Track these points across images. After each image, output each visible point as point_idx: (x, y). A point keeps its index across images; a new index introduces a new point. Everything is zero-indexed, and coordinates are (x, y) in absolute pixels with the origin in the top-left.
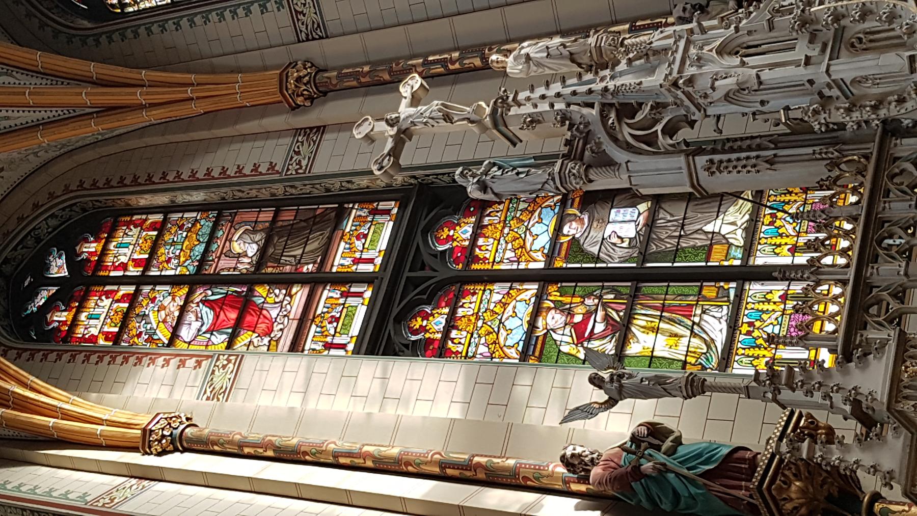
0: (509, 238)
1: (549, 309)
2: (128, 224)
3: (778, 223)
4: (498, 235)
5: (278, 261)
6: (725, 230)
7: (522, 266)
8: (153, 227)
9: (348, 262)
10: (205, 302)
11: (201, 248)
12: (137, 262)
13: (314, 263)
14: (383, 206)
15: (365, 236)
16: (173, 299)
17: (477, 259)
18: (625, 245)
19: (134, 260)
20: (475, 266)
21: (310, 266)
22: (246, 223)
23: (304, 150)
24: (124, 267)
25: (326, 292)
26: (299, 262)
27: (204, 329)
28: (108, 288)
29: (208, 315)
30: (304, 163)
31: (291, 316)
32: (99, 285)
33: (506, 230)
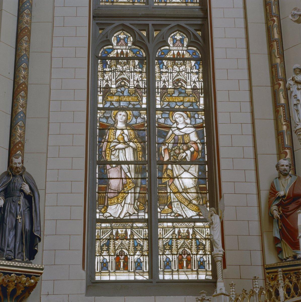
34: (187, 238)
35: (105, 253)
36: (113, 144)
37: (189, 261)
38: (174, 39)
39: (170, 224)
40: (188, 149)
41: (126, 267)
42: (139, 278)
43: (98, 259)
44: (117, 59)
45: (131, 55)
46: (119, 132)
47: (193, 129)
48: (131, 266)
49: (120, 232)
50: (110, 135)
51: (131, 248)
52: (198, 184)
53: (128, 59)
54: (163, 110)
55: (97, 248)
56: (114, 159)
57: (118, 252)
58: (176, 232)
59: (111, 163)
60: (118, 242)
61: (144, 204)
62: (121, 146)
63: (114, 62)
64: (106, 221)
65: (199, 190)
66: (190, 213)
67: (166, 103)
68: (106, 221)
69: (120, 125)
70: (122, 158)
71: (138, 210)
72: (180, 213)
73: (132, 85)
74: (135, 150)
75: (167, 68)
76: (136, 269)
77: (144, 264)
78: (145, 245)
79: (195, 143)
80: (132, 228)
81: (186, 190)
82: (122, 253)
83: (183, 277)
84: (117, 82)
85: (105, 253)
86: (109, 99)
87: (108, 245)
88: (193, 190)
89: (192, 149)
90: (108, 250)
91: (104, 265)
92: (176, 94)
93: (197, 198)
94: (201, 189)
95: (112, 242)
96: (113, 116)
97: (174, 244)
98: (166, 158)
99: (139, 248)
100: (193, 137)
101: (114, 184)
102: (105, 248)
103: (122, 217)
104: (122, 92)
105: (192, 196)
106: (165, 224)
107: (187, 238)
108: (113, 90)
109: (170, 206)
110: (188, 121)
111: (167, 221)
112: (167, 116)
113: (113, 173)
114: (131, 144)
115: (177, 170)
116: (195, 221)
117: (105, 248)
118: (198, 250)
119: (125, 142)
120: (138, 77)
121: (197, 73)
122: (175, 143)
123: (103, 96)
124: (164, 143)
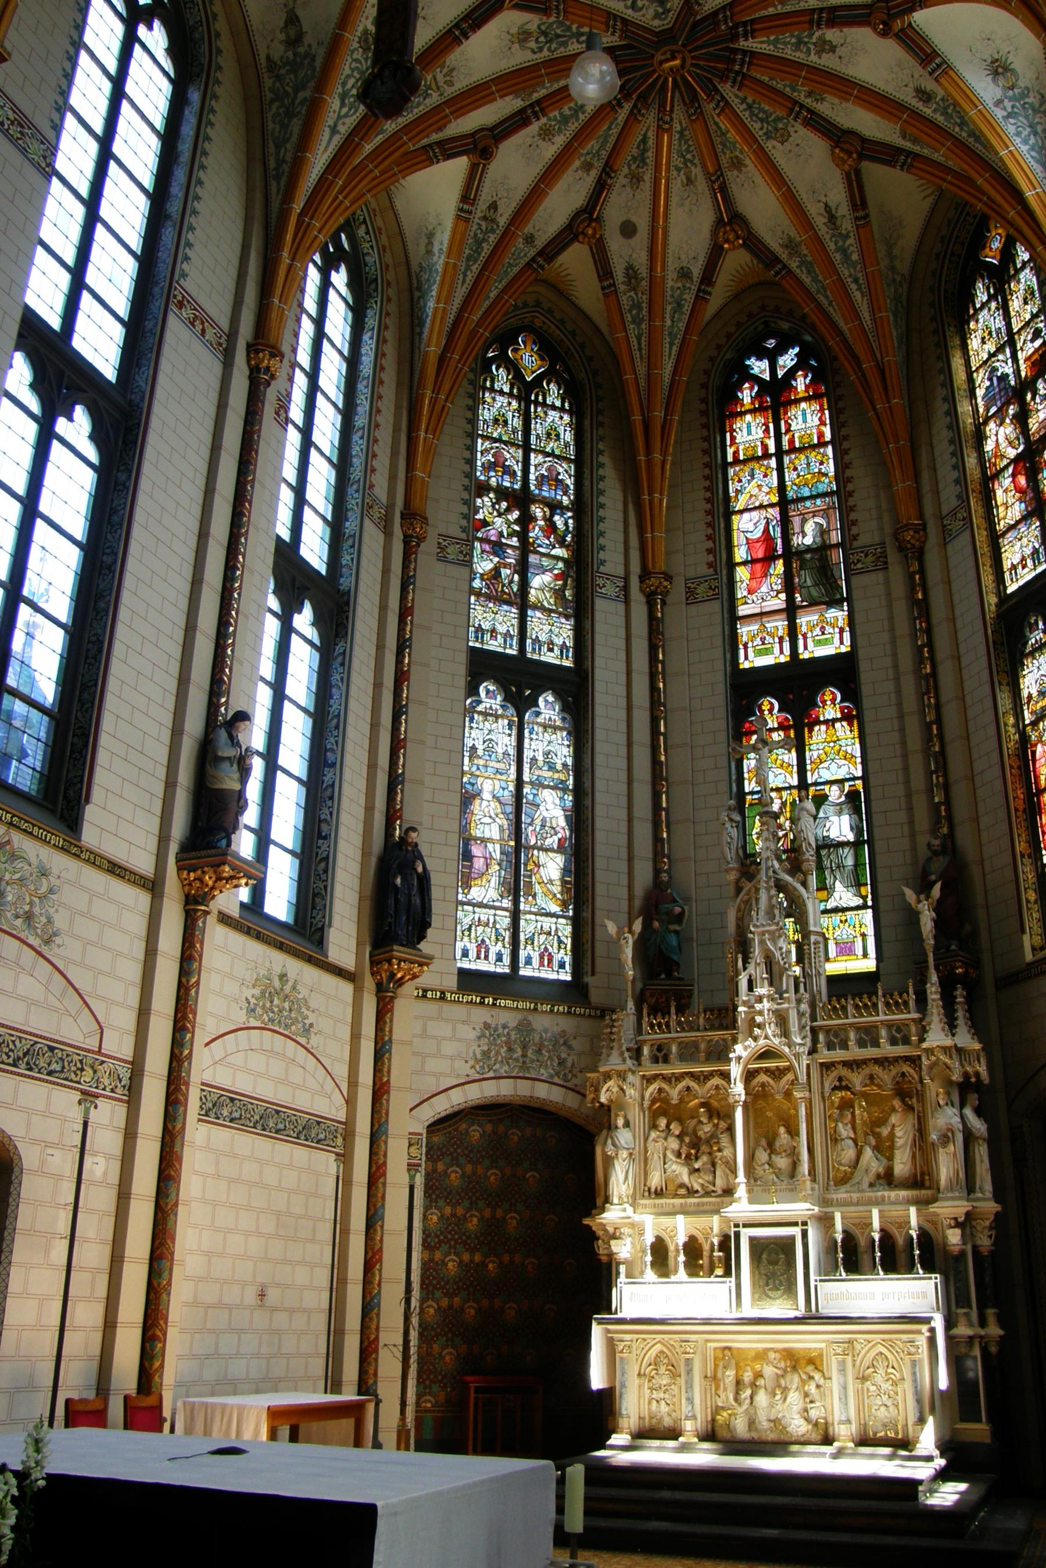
0: (827, 749)
1: (781, 798)
2: (822, 410)
3: (841, 925)
4: (829, 739)
5: (801, 568)
6: (836, 895)
7: (809, 767)
8: (821, 435)
9: (804, 629)
10: (767, 524)
11: (806, 492)
12: (792, 441)
13: (802, 601)
14: (847, 636)
15: (823, 633)
16: (767, 493)
17: (811, 731)
18: (825, 834)
19: (793, 436)
20: (806, 729)
21: (799, 599)
22: (828, 523)
23: (870, 558)
24: (788, 430)
25: (781, 623)
26: (801, 587)
27: (749, 535)
28: (771, 426)
29: (758, 534)
30: (859, 566)
31: (763, 604)
32: (773, 418)
33: (832, 744)
34: (549, 933)
35: (466, 939)
36: (478, 817)
37: (550, 961)
38: (546, 701)
39: (533, 917)
40: (556, 834)
41: (486, 958)
42: (499, 970)
43: (459, 945)
44: (485, 714)
45: (500, 712)
46: (485, 803)
47: (562, 813)
48: (492, 957)
49: (482, 918)
50: (477, 807)
51: (493, 938)
52: (563, 876)
53: (497, 717)
54: (531, 783)
55: (459, 933)
56: (479, 835)
57: (480, 939)
58: (539, 927)
59: (476, 839)
60: (480, 929)
61: (509, 892)
62: (487, 820)
63: (481, 718)
64: (469, 903)
65: (564, 883)
66: (555, 908)
67: (535, 777)
68: (469, 903)
69: (487, 795)
70: (487, 835)
71: (502, 896)
72: (543, 906)
73: (500, 750)
74: (501, 827)
75: (537, 734)
76: (497, 961)
77: (504, 957)
78: (507, 935)
79: (563, 829)
80: (495, 915)
81: (551, 882)
82: (483, 941)
83: (543, 975)
84: (484, 742)
85: (466, 939)
86: (476, 762)
87: (469, 929)
88: (558, 883)
89: (560, 836)
90: (469, 935)
91: (465, 954)
92: (546, 768)
93: (562, 893)
94: (566, 882)
95: (473, 928)
96: (479, 783)
97: (536, 939)
98: (532, 843)
99: (501, 939)
100: (562, 822)
101: (479, 864)
102: (466, 933)
103: (485, 902)
104: (490, 756)
105: (557, 889)
106: (528, 917)
107: (549, 933)
108: (480, 752)
109: (534, 896)
110: (557, 801)
111: (530, 913)
112: (535, 792)
113: (476, 850)
114: (497, 819)
115: (543, 857)
116: (558, 917)
117: (466, 933)
118: (559, 948)
119: (490, 817)
120: (507, 739)
121: (568, 746)
122: (543, 826)
123: (470, 757)
124: (530, 824)
